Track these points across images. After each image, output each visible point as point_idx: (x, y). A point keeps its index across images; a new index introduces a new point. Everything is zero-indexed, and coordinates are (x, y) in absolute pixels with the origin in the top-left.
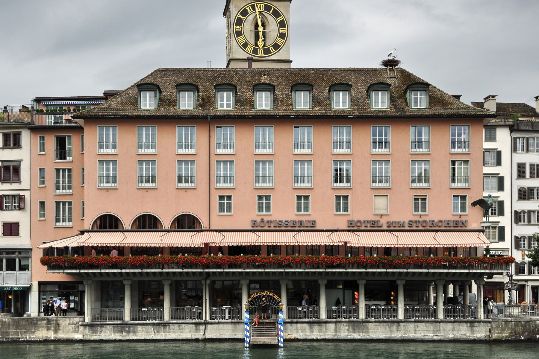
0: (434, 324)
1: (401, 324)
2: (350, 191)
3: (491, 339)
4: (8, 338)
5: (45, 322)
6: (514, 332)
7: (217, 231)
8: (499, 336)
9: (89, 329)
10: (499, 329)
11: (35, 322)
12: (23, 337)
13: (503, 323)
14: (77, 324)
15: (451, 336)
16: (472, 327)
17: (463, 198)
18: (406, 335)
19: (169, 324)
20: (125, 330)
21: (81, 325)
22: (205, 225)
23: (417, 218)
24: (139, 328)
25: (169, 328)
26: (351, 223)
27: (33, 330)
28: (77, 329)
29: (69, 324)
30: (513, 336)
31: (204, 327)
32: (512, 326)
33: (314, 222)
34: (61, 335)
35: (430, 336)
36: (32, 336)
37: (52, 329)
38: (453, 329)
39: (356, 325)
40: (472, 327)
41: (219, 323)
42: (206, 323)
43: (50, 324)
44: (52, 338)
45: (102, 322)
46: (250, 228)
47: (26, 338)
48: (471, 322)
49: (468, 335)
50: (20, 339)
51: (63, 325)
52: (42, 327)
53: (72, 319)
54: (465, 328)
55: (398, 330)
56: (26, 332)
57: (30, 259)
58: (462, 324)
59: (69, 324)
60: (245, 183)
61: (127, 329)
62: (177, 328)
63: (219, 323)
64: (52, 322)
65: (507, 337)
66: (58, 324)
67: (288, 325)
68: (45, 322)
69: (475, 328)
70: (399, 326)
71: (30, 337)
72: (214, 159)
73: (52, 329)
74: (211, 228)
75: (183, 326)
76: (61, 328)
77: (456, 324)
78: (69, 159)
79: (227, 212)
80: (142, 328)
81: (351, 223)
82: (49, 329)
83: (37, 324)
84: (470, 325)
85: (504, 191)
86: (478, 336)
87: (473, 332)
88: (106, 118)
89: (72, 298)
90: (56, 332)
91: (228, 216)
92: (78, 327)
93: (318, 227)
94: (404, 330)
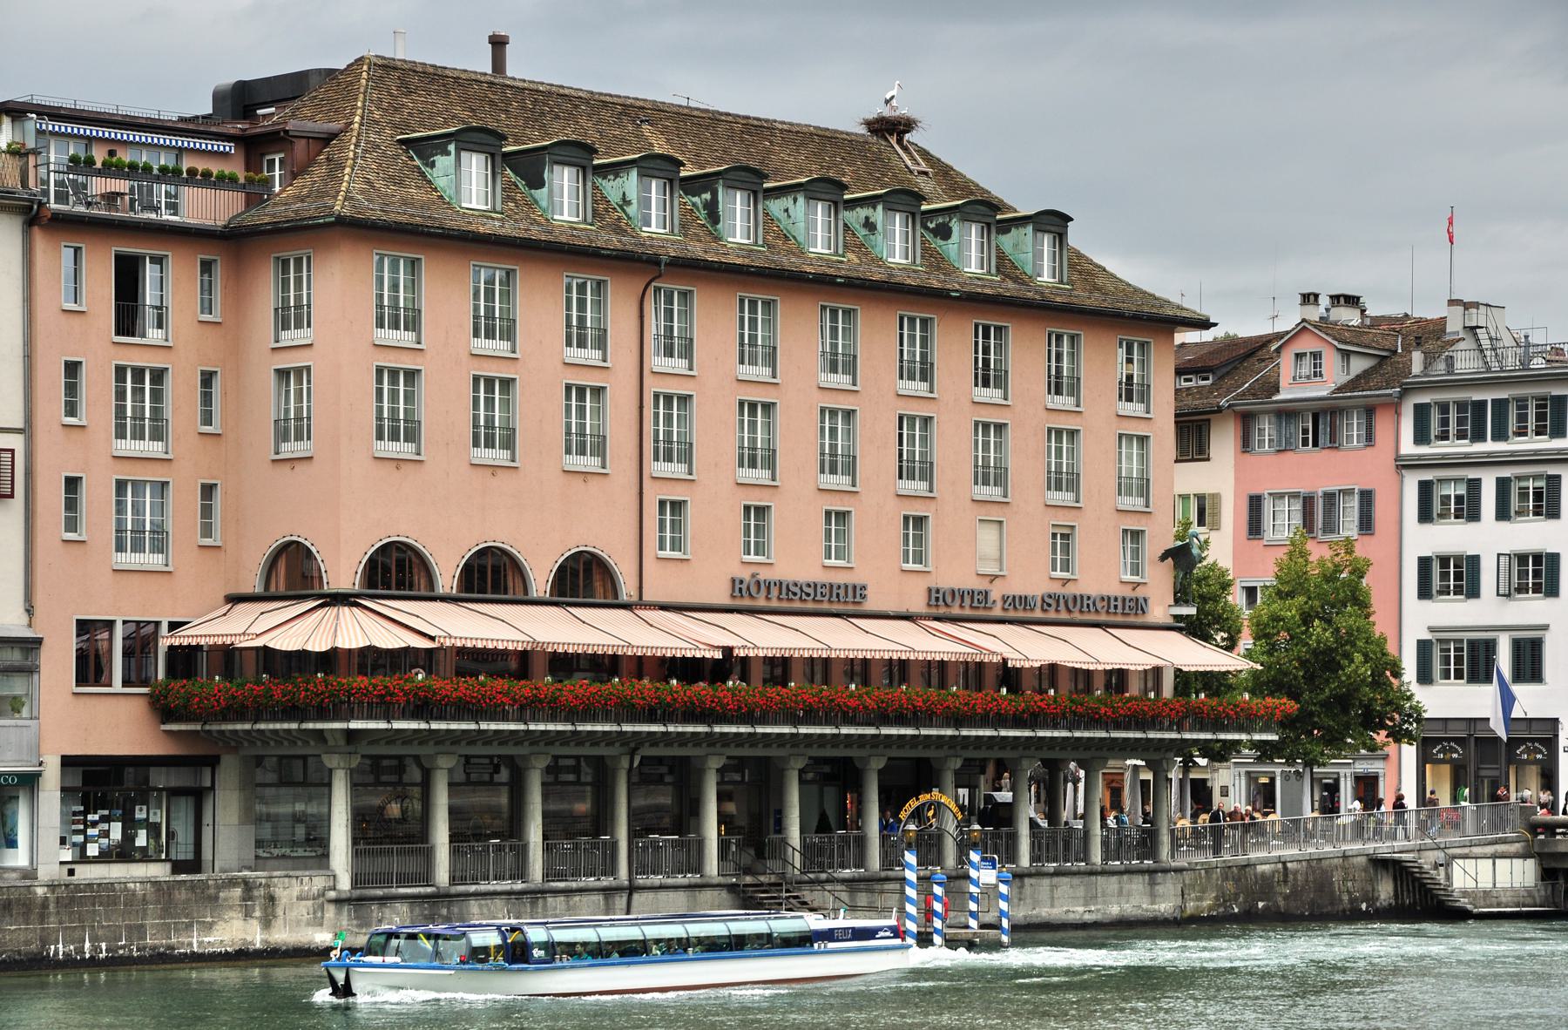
0: (1086, 879)
1: (1027, 881)
2: (932, 506)
3: (1185, 915)
4: (145, 948)
5: (238, 892)
6: (1223, 899)
7: (664, 607)
8: (1198, 907)
9: (349, 911)
10: (1197, 888)
11: (212, 891)
12: (183, 943)
13: (1203, 872)
14: (319, 896)
15: (1114, 910)
16: (1153, 884)
17: (1136, 535)
18: (1034, 912)
19: (543, 892)
20: (440, 916)
21: (330, 901)
22: (627, 591)
23: (1056, 589)
24: (474, 906)
25: (545, 907)
26: (936, 596)
27: (209, 919)
28: (319, 914)
29: (300, 898)
30: (1219, 906)
31: (625, 899)
32: (1217, 880)
34: (283, 936)
35: (1080, 912)
36: (206, 939)
37: (258, 914)
38: (1120, 893)
40: (1153, 884)
41: (662, 887)
42: (632, 889)
43: (250, 899)
44: (258, 946)
45: (386, 890)
47: (190, 944)
48: (1151, 872)
49: (1144, 906)
50: (173, 948)
51: (284, 901)
52: (231, 907)
53: (306, 879)
54: (1141, 887)
55: (1020, 899)
56: (189, 926)
57: (36, 677)
59: (300, 898)
60: (716, 465)
61: (444, 912)
62: (564, 906)
63: (662, 887)
64: (256, 893)
65: (1210, 908)
66: (272, 899)
68: (238, 892)
69: (1157, 887)
70: (1022, 887)
71: (200, 943)
72: (652, 386)
73: (258, 914)
74: (647, 597)
75: (577, 898)
76: (280, 912)
77: (1125, 877)
78: (154, 335)
79: (673, 549)
80: (480, 906)
81: (936, 596)
82: (248, 915)
83: (217, 898)
84: (1150, 879)
85: (1558, 555)
87: (1153, 897)
88: (422, 234)
89: (140, 814)
90: (267, 923)
91: (679, 563)
92: (322, 907)
93: (870, 605)
94: (1032, 897)
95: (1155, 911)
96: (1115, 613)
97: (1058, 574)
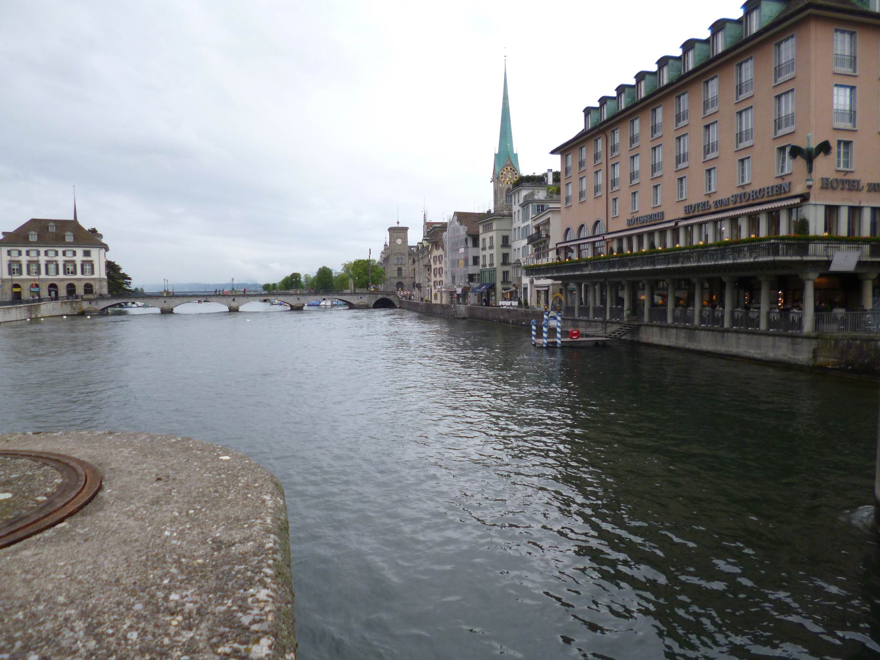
13: (833, 342)
16: (794, 344)
33: (662, 213)
38: (774, 346)
39: (692, 331)
46: (626, 227)
49: (789, 355)
58: (785, 340)
67: (648, 328)
70: (723, 336)
86: (800, 357)
95: (795, 359)
96: (772, 195)
97: (842, 168)
